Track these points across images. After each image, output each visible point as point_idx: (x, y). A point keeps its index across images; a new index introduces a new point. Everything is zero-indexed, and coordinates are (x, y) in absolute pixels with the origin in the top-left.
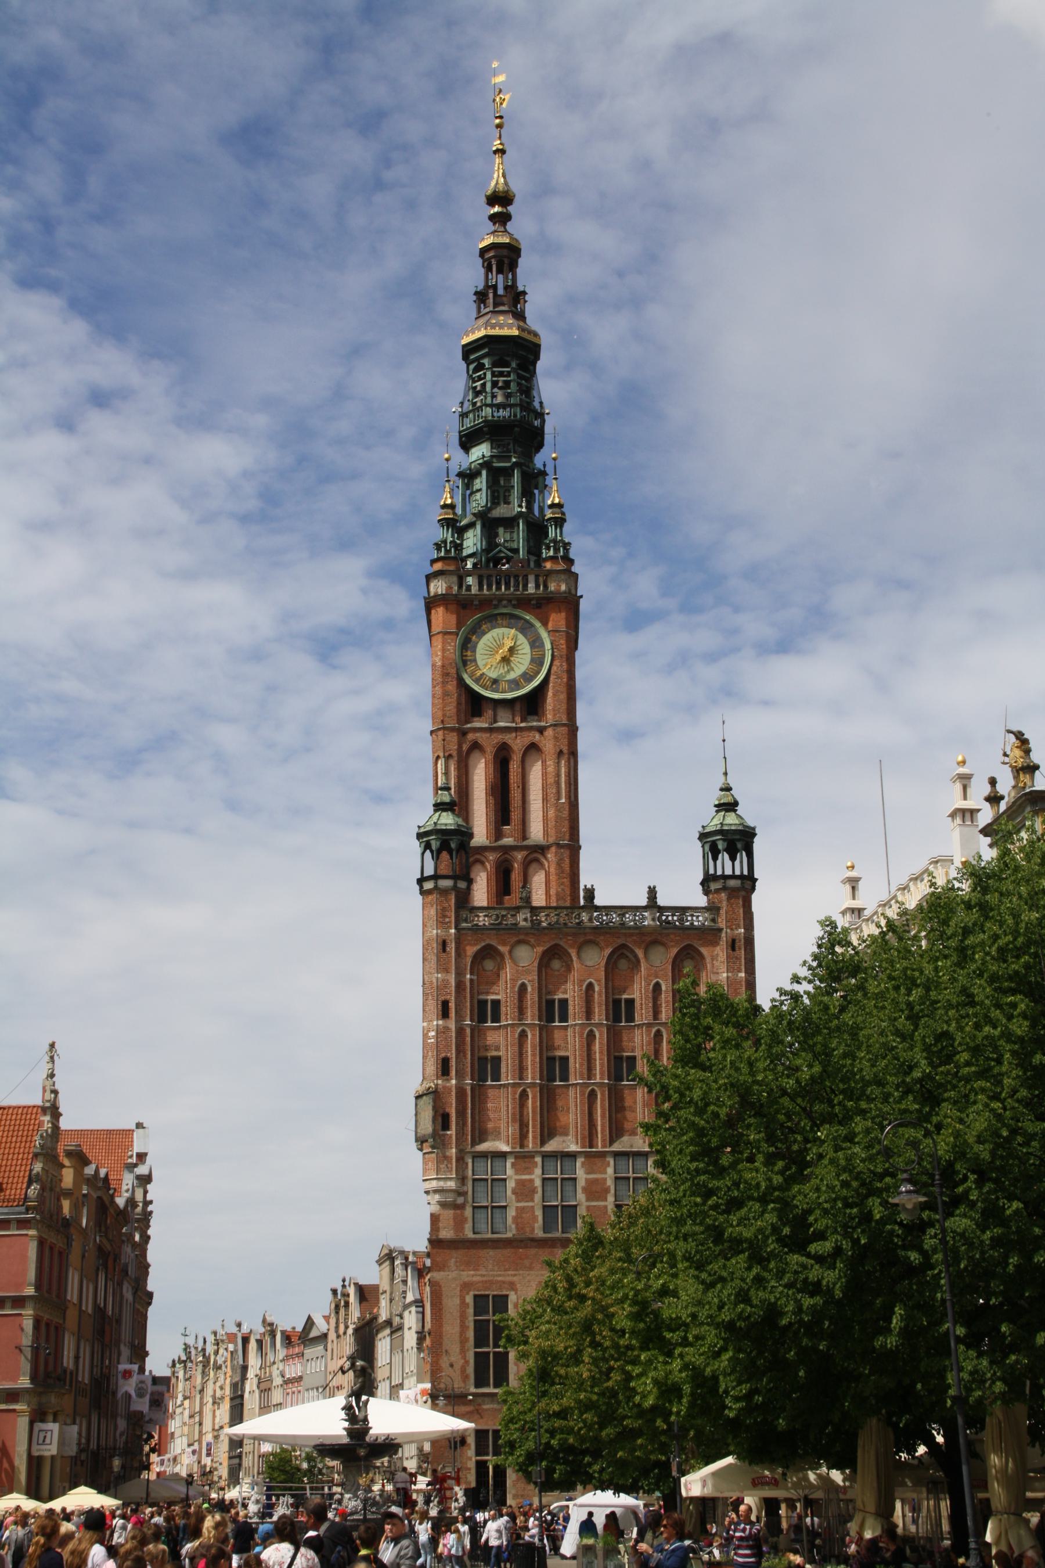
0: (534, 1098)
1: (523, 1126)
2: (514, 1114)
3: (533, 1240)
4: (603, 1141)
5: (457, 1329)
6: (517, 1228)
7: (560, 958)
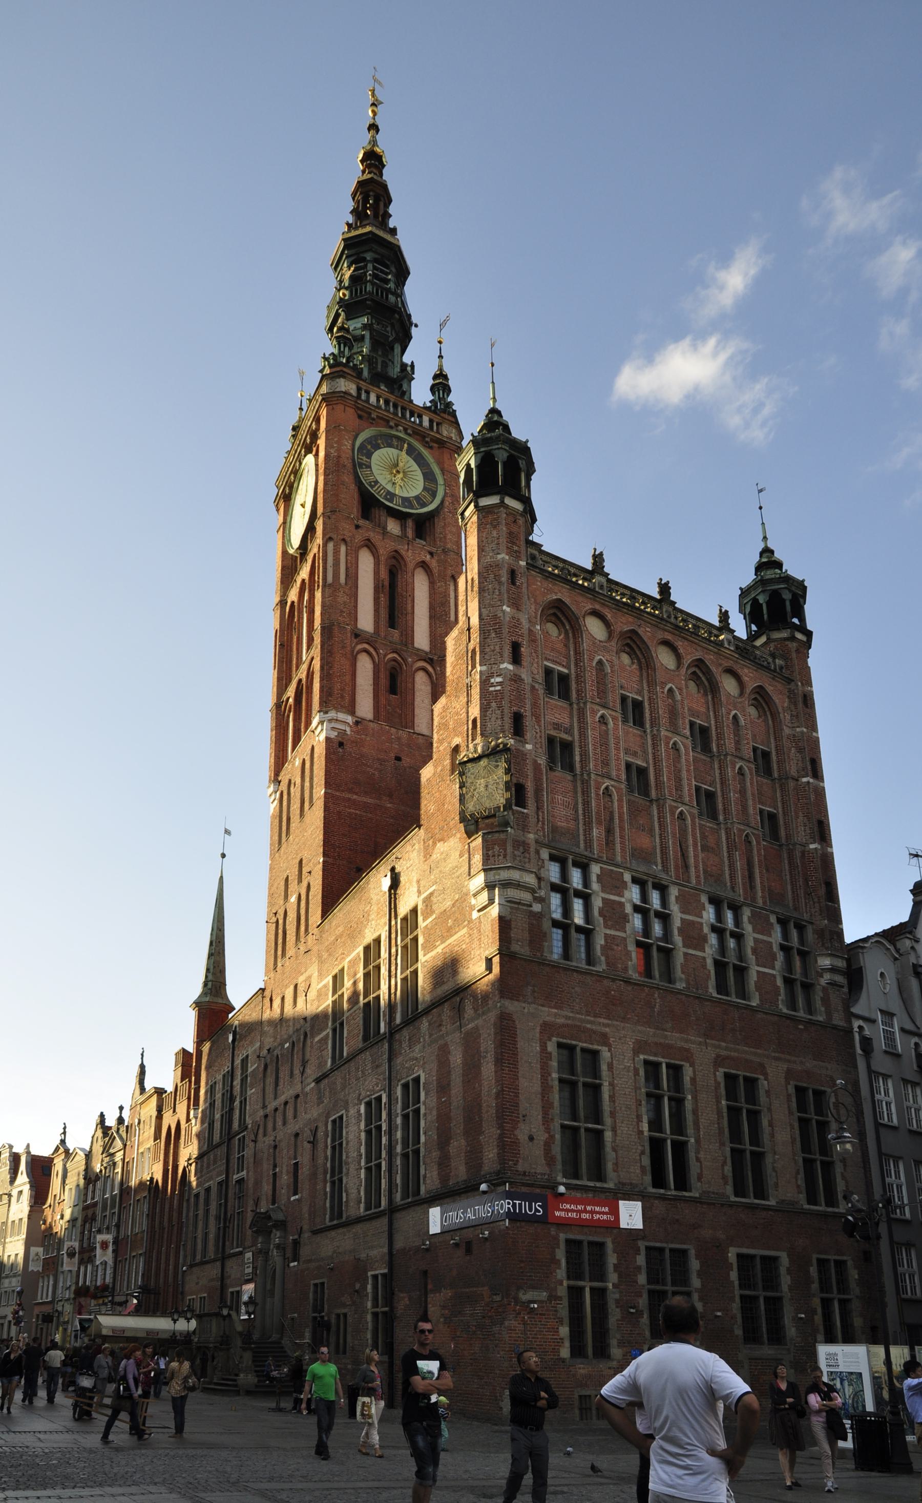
0: (620, 800)
1: (609, 831)
2: (598, 813)
3: (627, 981)
4: (698, 877)
5: (537, 1087)
6: (608, 964)
7: (632, 653)
